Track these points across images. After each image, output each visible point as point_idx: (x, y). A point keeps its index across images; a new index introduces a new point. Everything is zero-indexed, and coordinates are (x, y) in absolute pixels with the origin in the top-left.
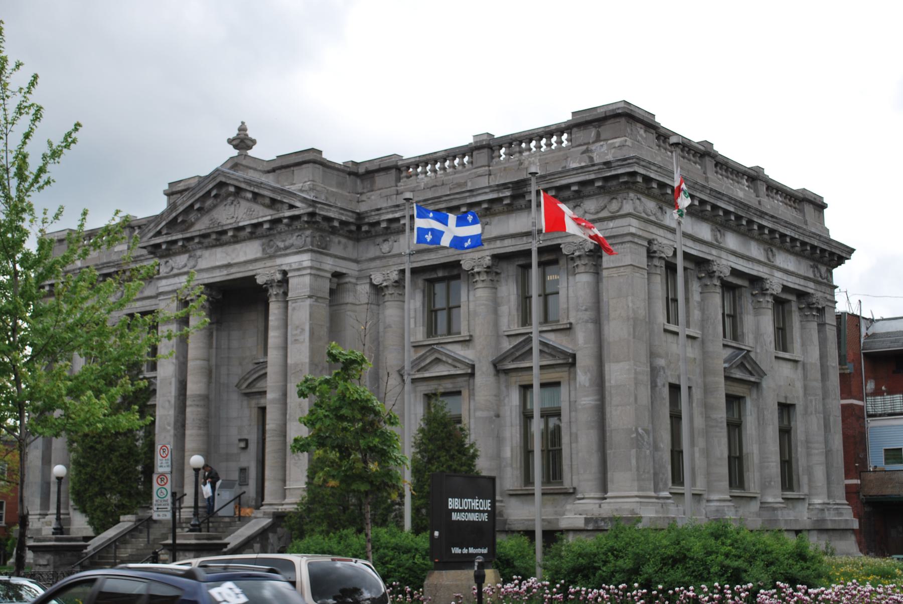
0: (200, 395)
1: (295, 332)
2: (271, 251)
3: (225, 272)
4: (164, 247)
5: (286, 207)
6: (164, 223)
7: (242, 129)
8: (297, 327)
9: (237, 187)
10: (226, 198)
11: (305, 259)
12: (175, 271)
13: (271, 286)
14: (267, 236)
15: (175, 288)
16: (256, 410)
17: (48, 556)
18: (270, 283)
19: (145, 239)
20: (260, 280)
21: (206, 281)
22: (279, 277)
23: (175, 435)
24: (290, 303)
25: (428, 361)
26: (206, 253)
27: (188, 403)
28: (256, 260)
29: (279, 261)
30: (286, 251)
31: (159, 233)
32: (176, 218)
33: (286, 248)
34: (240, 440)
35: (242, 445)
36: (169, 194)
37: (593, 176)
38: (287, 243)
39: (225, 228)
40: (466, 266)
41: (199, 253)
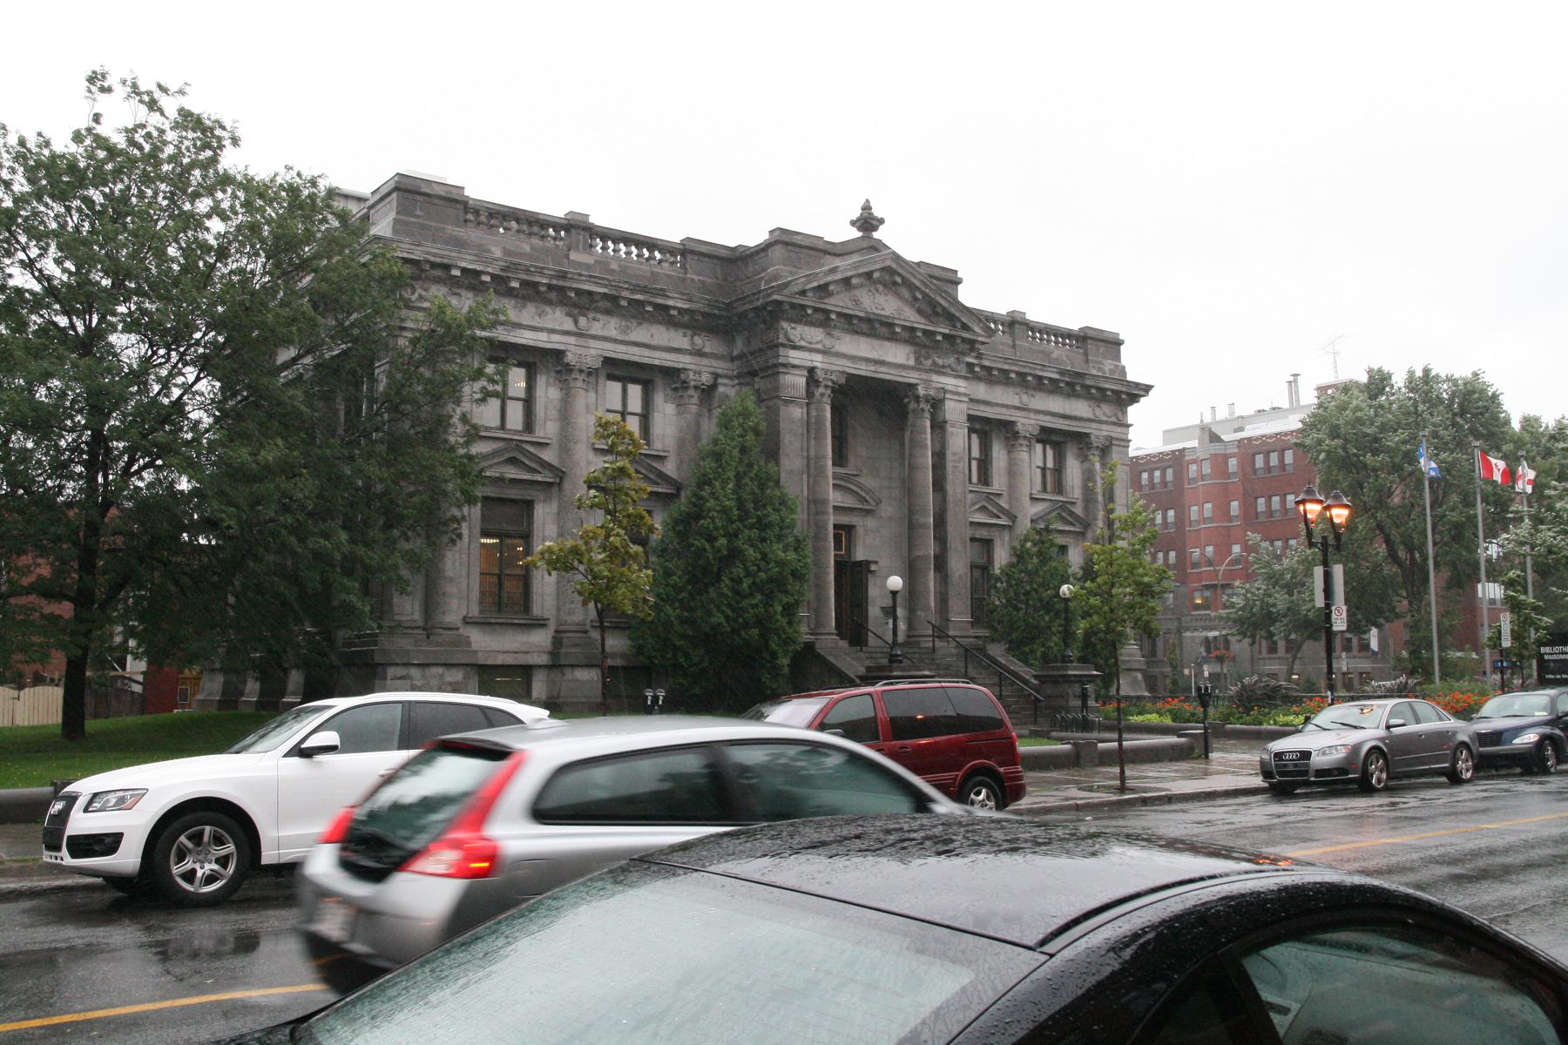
6: (815, 284)
7: (867, 207)
11: (962, 385)
12: (803, 343)
13: (927, 401)
15: (809, 364)
18: (928, 399)
20: (921, 391)
26: (847, 338)
28: (913, 368)
29: (935, 378)
30: (939, 370)
32: (827, 285)
40: (1019, 427)
41: (836, 333)
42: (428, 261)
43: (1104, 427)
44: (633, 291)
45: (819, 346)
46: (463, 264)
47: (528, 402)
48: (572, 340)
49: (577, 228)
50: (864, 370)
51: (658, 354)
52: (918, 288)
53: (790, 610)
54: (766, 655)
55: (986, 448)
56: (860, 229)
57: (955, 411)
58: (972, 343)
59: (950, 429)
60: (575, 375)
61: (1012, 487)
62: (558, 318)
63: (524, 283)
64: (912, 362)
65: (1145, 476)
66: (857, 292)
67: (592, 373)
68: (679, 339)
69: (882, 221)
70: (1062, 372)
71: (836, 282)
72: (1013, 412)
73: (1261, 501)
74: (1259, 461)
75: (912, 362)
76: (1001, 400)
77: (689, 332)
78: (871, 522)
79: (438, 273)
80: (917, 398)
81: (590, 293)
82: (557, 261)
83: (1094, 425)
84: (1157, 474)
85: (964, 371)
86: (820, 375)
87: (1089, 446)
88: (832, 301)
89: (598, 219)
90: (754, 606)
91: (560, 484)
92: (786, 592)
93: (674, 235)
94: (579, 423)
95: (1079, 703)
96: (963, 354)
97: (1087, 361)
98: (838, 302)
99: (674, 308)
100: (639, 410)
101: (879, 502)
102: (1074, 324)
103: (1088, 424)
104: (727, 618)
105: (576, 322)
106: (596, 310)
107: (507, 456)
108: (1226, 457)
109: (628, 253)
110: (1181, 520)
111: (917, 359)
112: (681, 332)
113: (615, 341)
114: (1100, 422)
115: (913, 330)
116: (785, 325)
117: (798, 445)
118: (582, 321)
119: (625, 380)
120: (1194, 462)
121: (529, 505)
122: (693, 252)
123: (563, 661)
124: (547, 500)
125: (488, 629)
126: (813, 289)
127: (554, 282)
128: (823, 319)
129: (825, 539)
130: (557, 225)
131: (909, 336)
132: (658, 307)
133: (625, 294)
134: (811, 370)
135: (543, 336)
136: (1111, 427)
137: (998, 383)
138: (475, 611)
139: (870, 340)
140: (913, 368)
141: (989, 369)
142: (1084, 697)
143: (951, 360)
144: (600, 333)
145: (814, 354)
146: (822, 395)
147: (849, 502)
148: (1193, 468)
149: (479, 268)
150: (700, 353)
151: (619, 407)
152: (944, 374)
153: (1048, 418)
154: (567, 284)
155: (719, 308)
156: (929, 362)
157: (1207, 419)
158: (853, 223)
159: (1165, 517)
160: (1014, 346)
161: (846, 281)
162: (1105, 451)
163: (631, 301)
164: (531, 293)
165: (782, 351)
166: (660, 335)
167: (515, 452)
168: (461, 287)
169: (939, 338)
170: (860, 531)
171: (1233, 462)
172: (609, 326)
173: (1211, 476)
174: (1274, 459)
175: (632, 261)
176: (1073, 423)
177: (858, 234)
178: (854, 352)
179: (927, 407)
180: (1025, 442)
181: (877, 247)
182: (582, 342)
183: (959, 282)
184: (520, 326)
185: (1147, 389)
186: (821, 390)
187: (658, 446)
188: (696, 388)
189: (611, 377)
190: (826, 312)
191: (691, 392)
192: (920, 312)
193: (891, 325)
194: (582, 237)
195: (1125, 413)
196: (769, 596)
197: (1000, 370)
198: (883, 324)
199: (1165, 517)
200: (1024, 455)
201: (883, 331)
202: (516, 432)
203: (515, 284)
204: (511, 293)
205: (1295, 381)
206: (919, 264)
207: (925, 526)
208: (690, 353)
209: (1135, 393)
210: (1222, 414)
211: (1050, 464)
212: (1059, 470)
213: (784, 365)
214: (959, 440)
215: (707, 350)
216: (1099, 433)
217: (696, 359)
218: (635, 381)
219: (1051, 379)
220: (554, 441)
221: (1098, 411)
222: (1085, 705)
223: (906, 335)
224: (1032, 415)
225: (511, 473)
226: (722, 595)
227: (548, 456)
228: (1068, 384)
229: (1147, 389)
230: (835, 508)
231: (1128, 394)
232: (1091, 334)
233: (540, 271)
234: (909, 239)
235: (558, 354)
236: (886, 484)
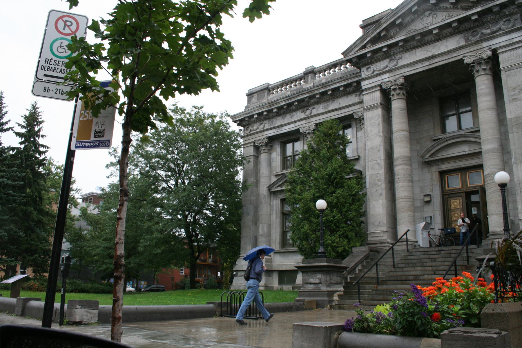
0: (407, 157)
1: (513, 93)
2: (473, 39)
3: (427, 64)
4: (369, 55)
8: (514, 89)
12: (377, 72)
13: (480, 64)
14: (470, 29)
15: (379, 83)
16: (437, 174)
17: (319, 276)
19: (352, 53)
20: (467, 61)
21: (408, 74)
22: (489, 53)
23: (386, 188)
24: (502, 73)
27: (395, 163)
29: (485, 44)
31: (364, 47)
32: (379, 33)
34: (425, 196)
35: (427, 199)
36: (362, 27)
38: (494, 29)
39: (430, 28)
41: (398, 57)
42: (246, 117)
46: (256, 112)
48: (304, 122)
51: (342, 111)
60: (308, 136)
62: (299, 115)
75: (463, 43)
77: (358, 93)
79: (253, 119)
81: (302, 100)
99: (341, 86)
106: (313, 104)
107: (284, 180)
111: (467, 40)
112: (354, 95)
115: (449, 25)
118: (308, 112)
125: (282, 254)
127: (287, 102)
128: (376, 56)
132: (333, 90)
133: (316, 92)
134: (380, 86)
135: (292, 125)
139: (424, 48)
143: (501, 24)
149: (261, 111)
172: (320, 109)
178: (412, 61)
182: (308, 121)
186: (392, 93)
193: (431, 31)
201: (429, 38)
203: (275, 110)
204: (278, 114)
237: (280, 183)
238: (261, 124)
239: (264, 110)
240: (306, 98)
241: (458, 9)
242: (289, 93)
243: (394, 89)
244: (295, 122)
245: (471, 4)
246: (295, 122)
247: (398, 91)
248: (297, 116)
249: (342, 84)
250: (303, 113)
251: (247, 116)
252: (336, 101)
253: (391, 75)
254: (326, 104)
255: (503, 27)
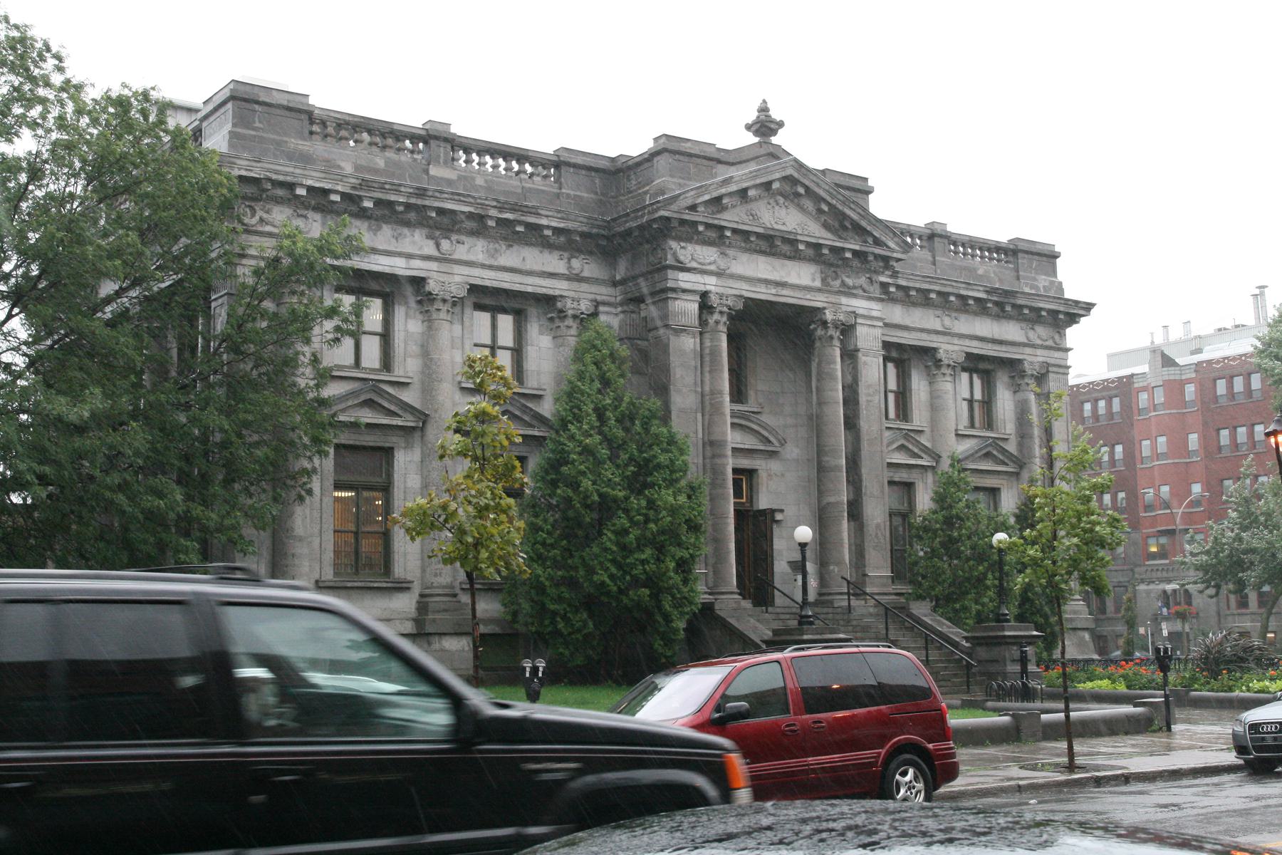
3: (773, 291)
5: (870, 240)
6: (707, 197)
7: (764, 109)
8: (869, 386)
9: (807, 188)
10: (773, 195)
11: (875, 308)
12: (694, 265)
14: (831, 265)
15: (702, 288)
24: (860, 355)
25: (895, 446)
26: (745, 257)
28: (819, 290)
29: (844, 300)
33: (855, 287)
37: (1062, 309)
39: (799, 238)
40: (941, 354)
41: (731, 252)
42: (269, 179)
43: (1039, 352)
44: (501, 209)
45: (713, 268)
46: (310, 182)
47: (386, 337)
48: (434, 266)
49: (435, 139)
50: (764, 293)
51: (530, 280)
52: (824, 200)
53: (684, 566)
54: (659, 618)
55: (903, 378)
56: (756, 133)
57: (868, 339)
58: (886, 260)
59: (862, 358)
60: (438, 305)
61: (934, 422)
63: (378, 203)
64: (818, 284)
65: (1088, 406)
66: (753, 206)
67: (457, 303)
68: (554, 262)
69: (781, 124)
70: (991, 291)
71: (730, 194)
72: (934, 337)
73: (1225, 433)
74: (1221, 387)
75: (818, 284)
76: (920, 324)
77: (566, 255)
78: (774, 466)
79: (280, 192)
80: (824, 324)
81: (453, 212)
82: (412, 177)
83: (1028, 350)
84: (1102, 404)
85: (876, 291)
86: (714, 301)
87: (1022, 374)
88: (726, 215)
89: (460, 129)
90: (643, 562)
91: (422, 429)
92: (679, 545)
93: (546, 145)
94: (442, 358)
95: (1017, 668)
96: (876, 272)
97: (1018, 278)
98: (733, 217)
99: (548, 227)
100: (511, 344)
101: (783, 443)
102: (1001, 234)
103: (1021, 350)
104: (612, 577)
105: (438, 246)
106: (459, 231)
107: (363, 398)
108: (1182, 384)
109: (495, 167)
110: (1131, 456)
111: (823, 280)
112: (556, 254)
113: (483, 266)
114: (1033, 346)
116: (673, 244)
117: (689, 379)
118: (445, 244)
119: (495, 310)
120: (1144, 389)
121: (388, 452)
122: (568, 164)
123: (429, 629)
124: (409, 446)
125: (344, 592)
126: (706, 203)
127: (413, 201)
129: (723, 486)
130: (415, 138)
131: (816, 253)
132: (529, 226)
133: (493, 212)
134: (704, 295)
136: (1045, 352)
137: (914, 304)
138: (329, 574)
139: (770, 259)
140: (819, 290)
141: (906, 289)
142: (1023, 660)
143: (862, 281)
144: (465, 257)
145: (710, 276)
146: (717, 322)
147: (749, 442)
148: (1144, 396)
150: (578, 278)
151: (489, 342)
152: (855, 296)
153: (975, 343)
154: (427, 203)
155: (599, 227)
156: (838, 283)
157: (1159, 340)
158: (748, 127)
159: (1112, 453)
160: (934, 264)
161: (743, 193)
162: (1041, 378)
163: (501, 222)
164: (388, 213)
165: (671, 274)
166: (533, 258)
167: (373, 393)
168: (307, 208)
169: (848, 255)
170: (763, 475)
171: (1190, 389)
172: (475, 249)
173: (1165, 405)
174: (1239, 384)
175: (500, 176)
176: (1004, 348)
177: (752, 139)
179: (836, 334)
180: (949, 371)
181: (776, 154)
182: (445, 267)
183: (868, 191)
184: (374, 251)
185: (1088, 307)
186: (716, 316)
187: (532, 384)
188: (575, 317)
189: (479, 307)
190: (722, 228)
191: (569, 322)
192: (826, 226)
193: (793, 242)
194: (442, 150)
195: (1062, 336)
196: (661, 549)
197: (918, 290)
198: (786, 240)
199: (1112, 453)
200: (946, 386)
201: (786, 248)
202: (373, 370)
203: (368, 204)
204: (362, 214)
205: (1262, 294)
206: (824, 172)
207: (838, 468)
208: (568, 278)
209: (1074, 312)
210: (1176, 334)
211: (978, 395)
212: (988, 403)
213: (674, 290)
214: (873, 369)
215: (586, 274)
216: (1033, 359)
217: (575, 285)
218: (505, 311)
219: (976, 299)
220: (416, 380)
221: (1031, 334)
222: (1024, 671)
223: (811, 252)
224: (956, 341)
225: (367, 416)
226: (606, 550)
227: (408, 396)
228: (996, 303)
229: (1088, 307)
230: (735, 450)
231: (1067, 314)
232: (1022, 246)
233: (396, 189)
234: (811, 144)
235: (418, 282)
236: (790, 421)
237: (350, 403)
238: (299, 216)
239: (339, 188)
240: (463, 213)
241: (817, 219)
242: (380, 163)
243: (721, 313)
244: (410, 256)
245: (837, 225)
246: (410, 256)
247: (725, 319)
248: (414, 243)
249: (554, 224)
250: (431, 243)
251: (274, 177)
252: (516, 247)
253: (720, 283)
254: (491, 246)
255: (865, 286)
